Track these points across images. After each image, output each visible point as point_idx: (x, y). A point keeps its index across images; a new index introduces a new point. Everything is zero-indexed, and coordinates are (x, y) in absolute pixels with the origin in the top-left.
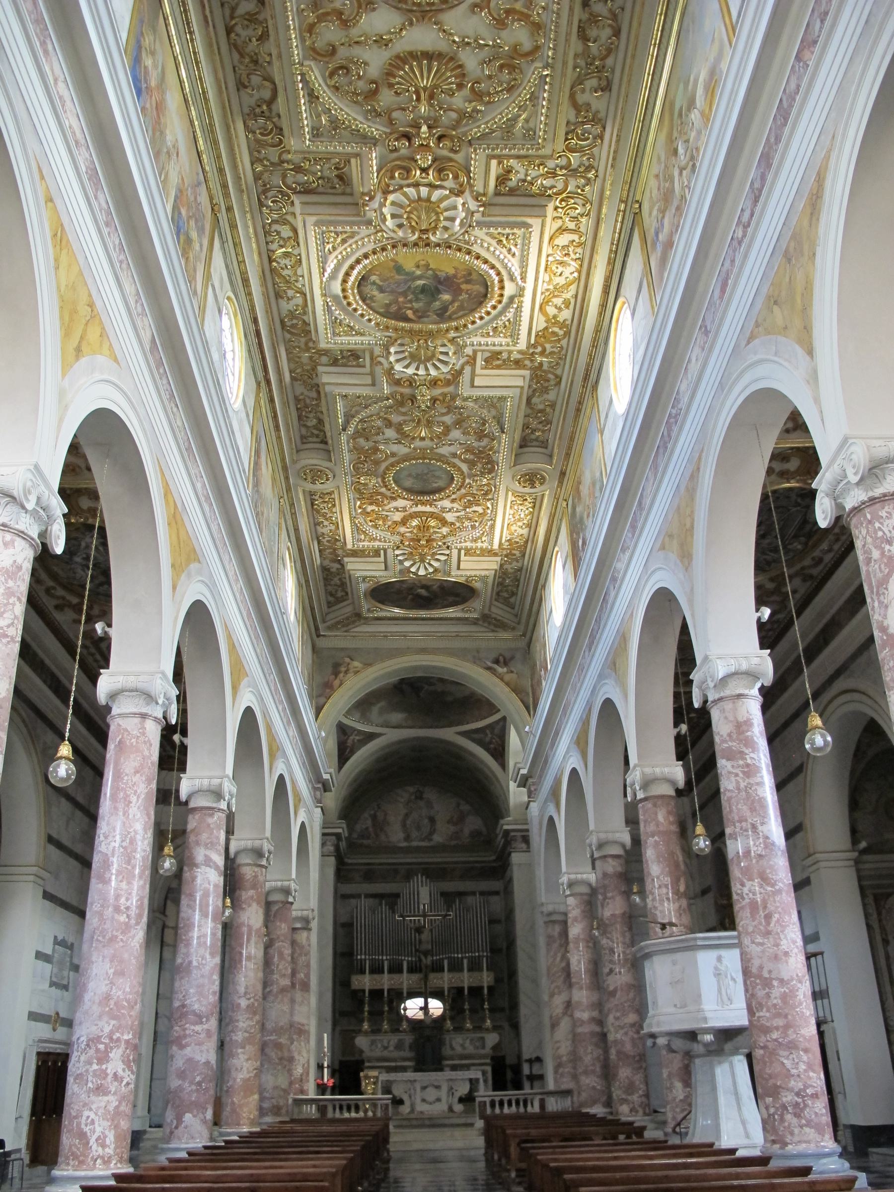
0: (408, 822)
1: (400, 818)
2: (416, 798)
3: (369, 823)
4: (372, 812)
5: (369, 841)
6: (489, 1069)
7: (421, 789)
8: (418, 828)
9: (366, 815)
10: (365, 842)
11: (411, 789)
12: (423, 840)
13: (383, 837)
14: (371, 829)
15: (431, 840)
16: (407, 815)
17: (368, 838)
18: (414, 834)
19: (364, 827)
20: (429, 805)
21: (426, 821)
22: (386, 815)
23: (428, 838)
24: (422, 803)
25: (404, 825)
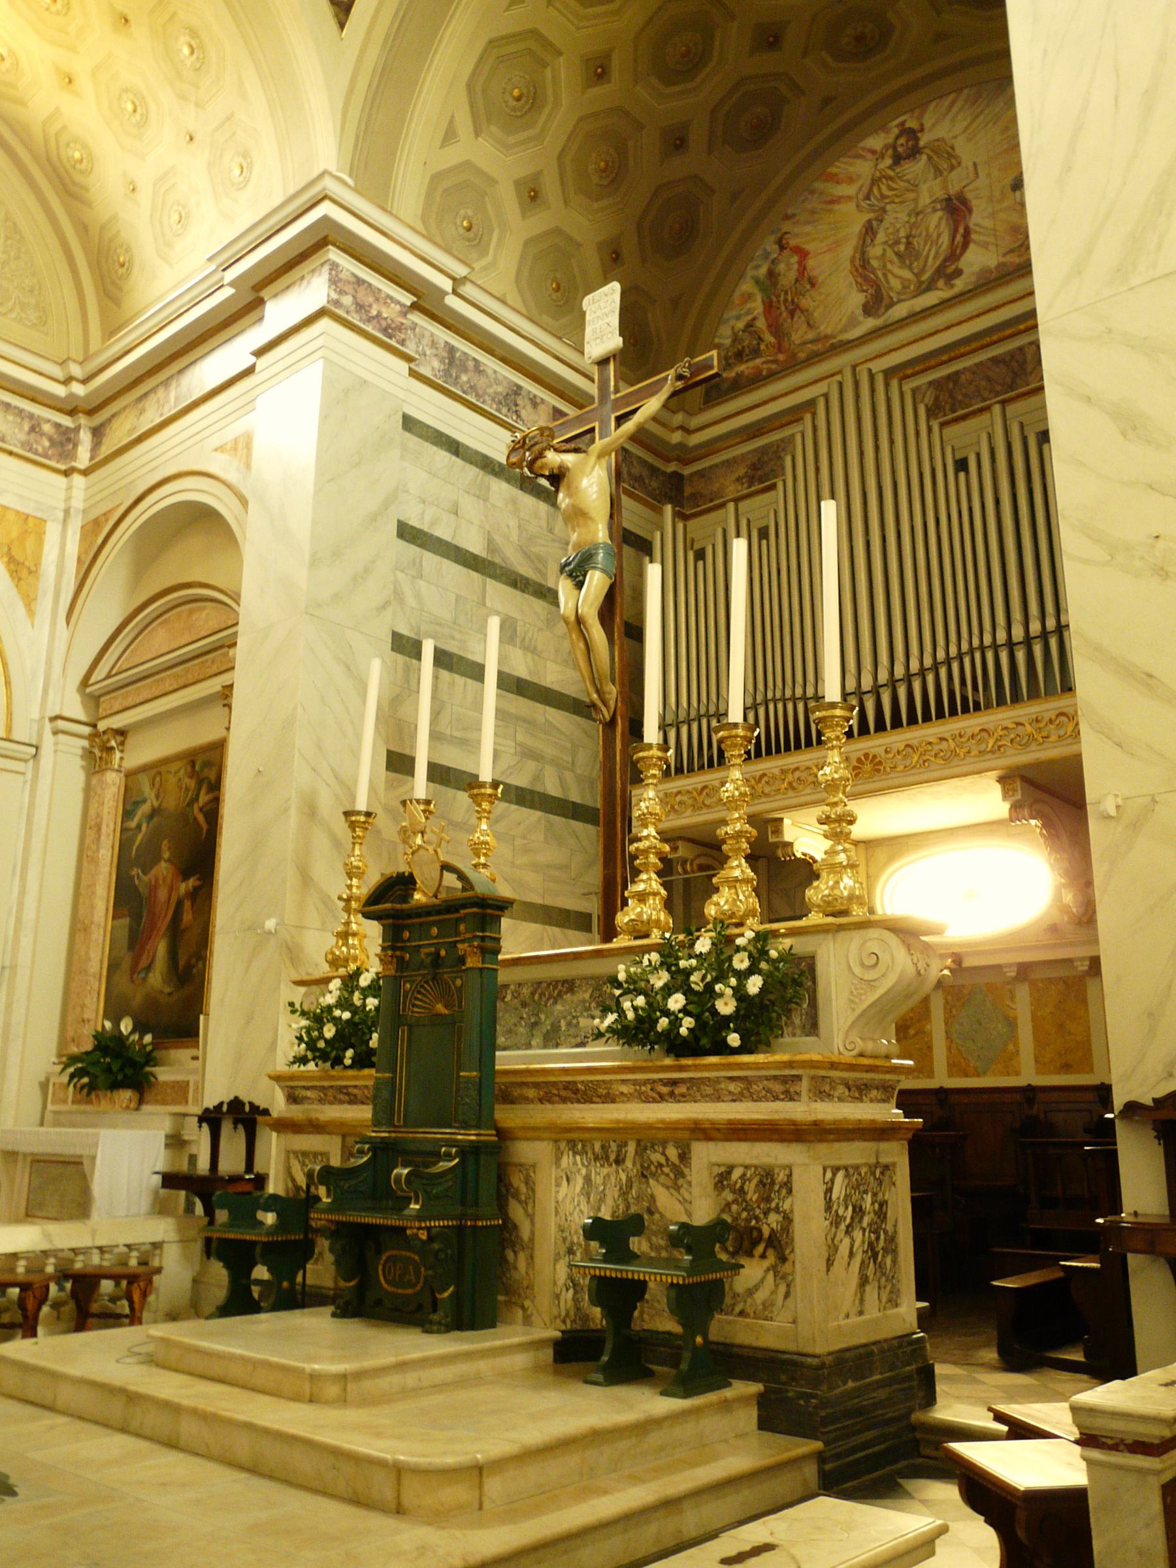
0: (875, 251)
1: (848, 251)
2: (897, 160)
3: (757, 305)
4: (763, 270)
5: (758, 361)
6: (898, 1155)
7: (912, 124)
8: (908, 254)
9: (747, 286)
10: (743, 368)
11: (876, 142)
12: (930, 286)
13: (799, 334)
14: (761, 324)
15: (958, 273)
16: (869, 231)
17: (756, 353)
18: (897, 276)
19: (740, 325)
20: (946, 158)
21: (936, 221)
22: (802, 254)
23: (947, 271)
24: (917, 168)
25: (862, 267)
